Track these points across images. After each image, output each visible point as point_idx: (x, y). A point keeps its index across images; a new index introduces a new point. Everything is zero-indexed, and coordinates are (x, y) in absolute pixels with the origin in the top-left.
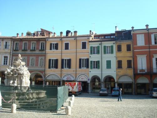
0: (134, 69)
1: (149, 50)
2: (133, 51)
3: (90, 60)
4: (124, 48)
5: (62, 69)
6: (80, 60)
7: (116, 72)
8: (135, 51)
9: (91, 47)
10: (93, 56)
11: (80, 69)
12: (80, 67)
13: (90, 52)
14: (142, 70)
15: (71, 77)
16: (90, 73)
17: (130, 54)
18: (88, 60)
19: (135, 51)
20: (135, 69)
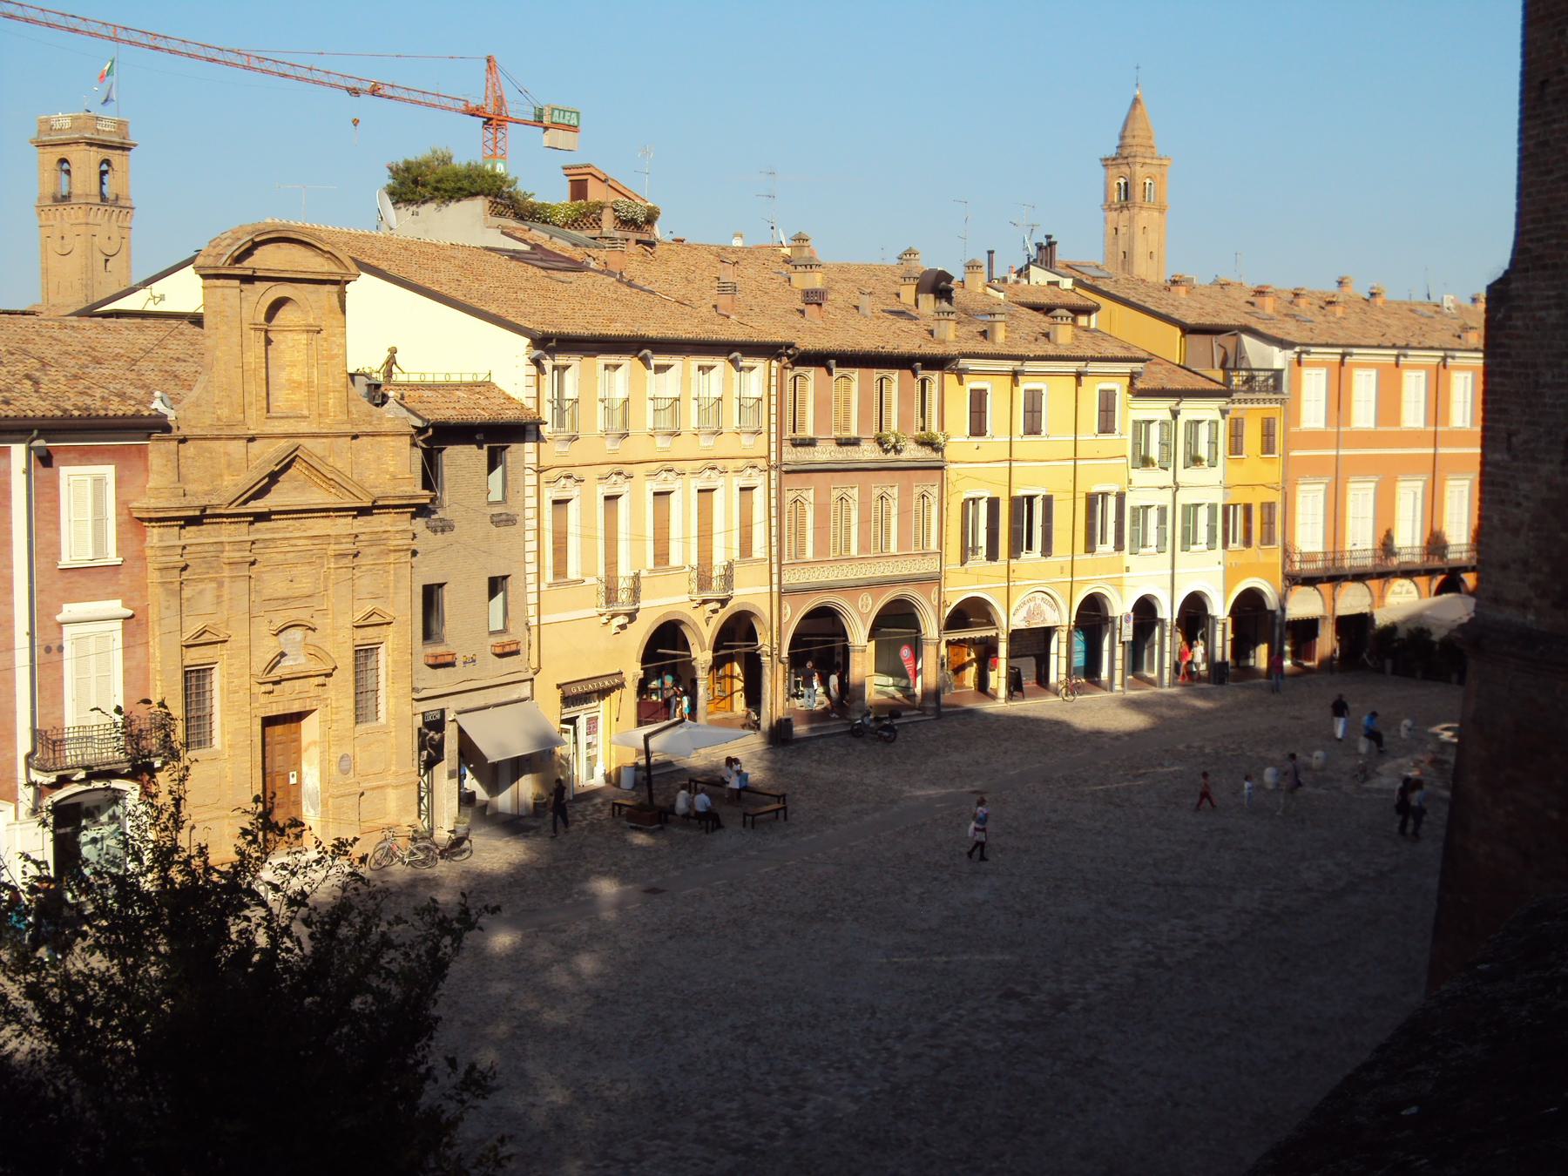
0: (1285, 551)
1: (1334, 453)
2: (1286, 452)
3: (1130, 502)
4: (1252, 437)
5: (1013, 562)
6: (1091, 500)
7: (1221, 568)
8: (1294, 453)
9: (1135, 422)
10: (1141, 476)
11: (1089, 556)
12: (1090, 547)
13: (1129, 454)
14: (1309, 558)
15: (1045, 607)
16: (1125, 574)
17: (1271, 471)
18: (1121, 498)
19: (1294, 453)
20: (1287, 554)
